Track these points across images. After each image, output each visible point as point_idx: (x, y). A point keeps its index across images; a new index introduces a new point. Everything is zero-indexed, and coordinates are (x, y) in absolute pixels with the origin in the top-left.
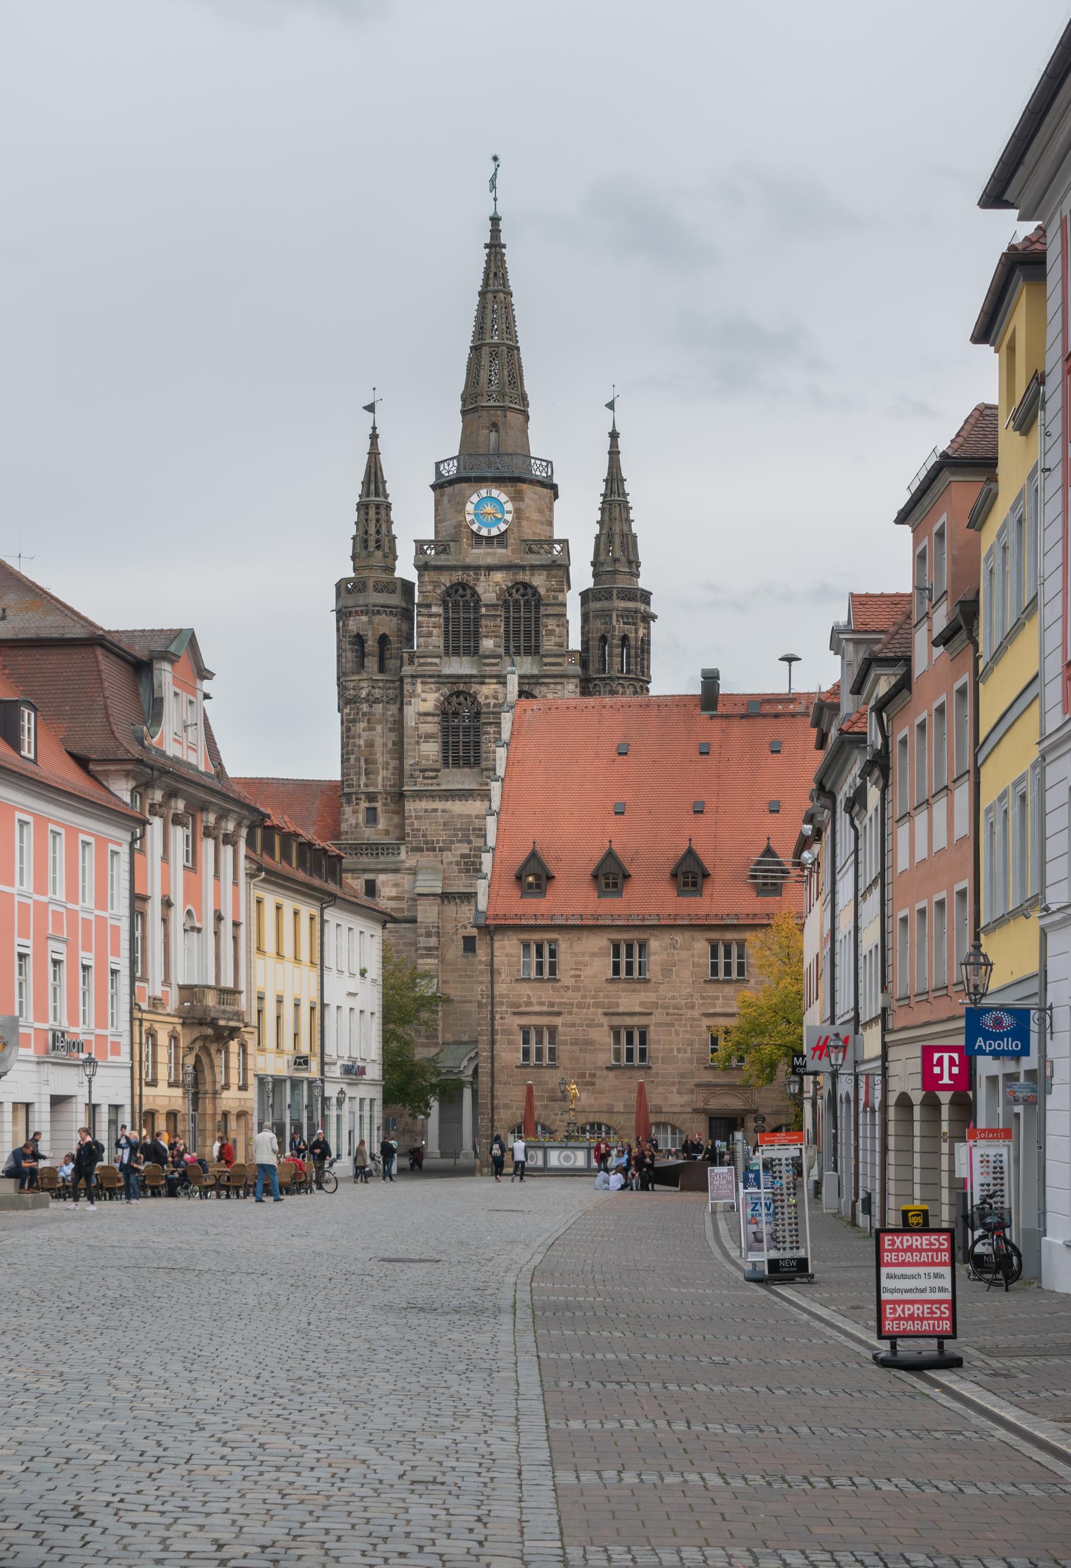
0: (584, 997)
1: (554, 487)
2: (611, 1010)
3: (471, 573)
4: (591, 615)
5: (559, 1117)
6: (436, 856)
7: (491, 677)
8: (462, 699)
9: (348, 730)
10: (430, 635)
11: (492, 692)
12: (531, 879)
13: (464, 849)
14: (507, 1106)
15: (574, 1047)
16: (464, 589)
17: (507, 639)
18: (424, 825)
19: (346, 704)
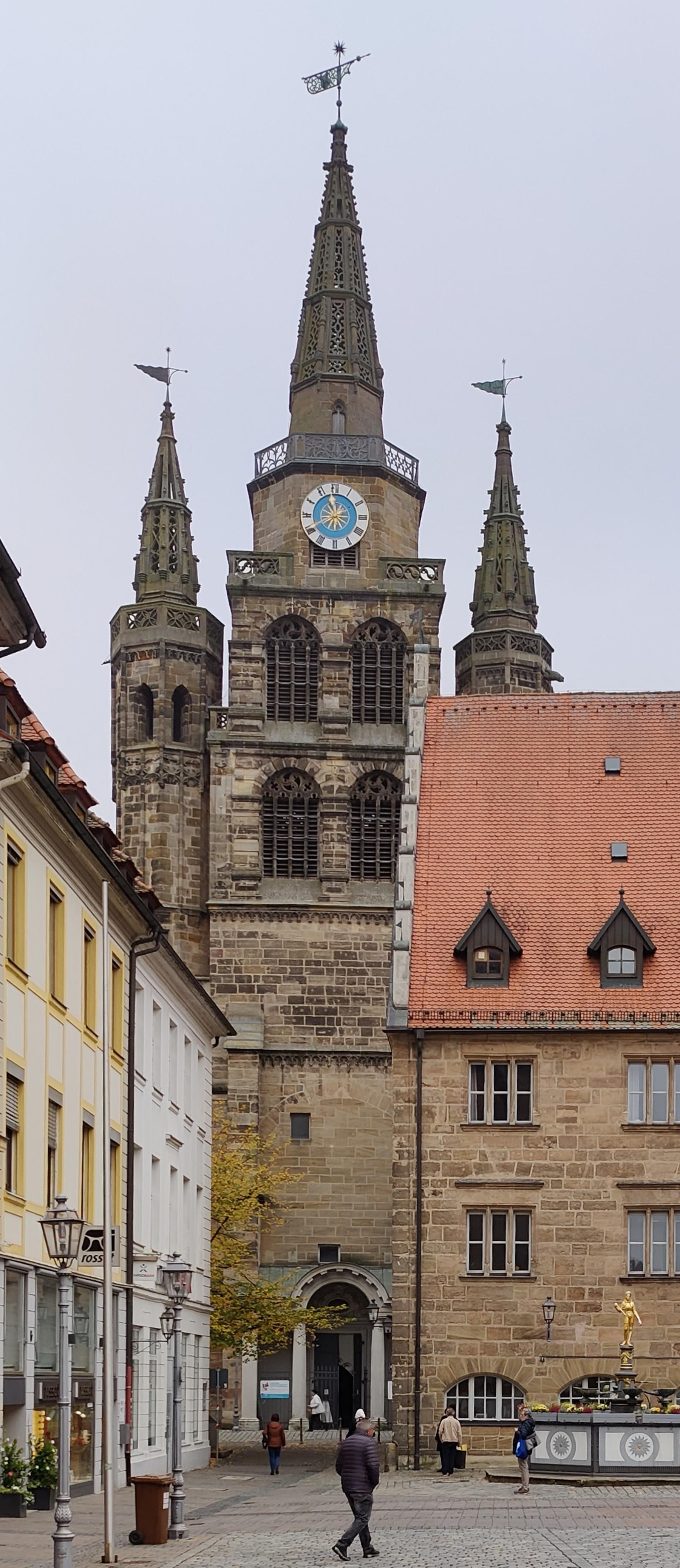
0: (581, 1156)
1: (421, 495)
2: (630, 1180)
3: (309, 602)
4: (474, 671)
5: (535, 1367)
6: (254, 1000)
7: (335, 748)
8: (292, 779)
9: (129, 821)
10: (249, 687)
11: (336, 771)
12: (482, 956)
13: (294, 989)
14: (442, 1347)
15: (563, 1244)
16: (297, 627)
17: (357, 700)
18: (237, 956)
19: (126, 783)
